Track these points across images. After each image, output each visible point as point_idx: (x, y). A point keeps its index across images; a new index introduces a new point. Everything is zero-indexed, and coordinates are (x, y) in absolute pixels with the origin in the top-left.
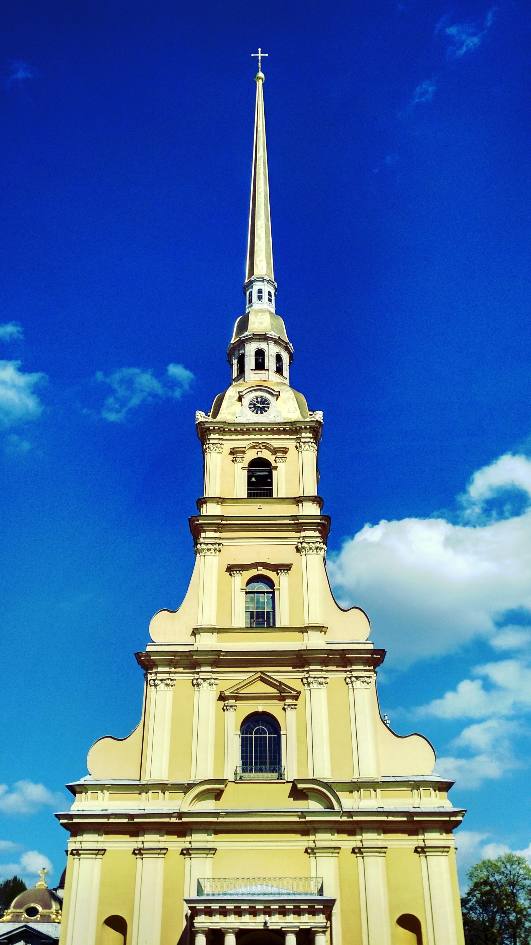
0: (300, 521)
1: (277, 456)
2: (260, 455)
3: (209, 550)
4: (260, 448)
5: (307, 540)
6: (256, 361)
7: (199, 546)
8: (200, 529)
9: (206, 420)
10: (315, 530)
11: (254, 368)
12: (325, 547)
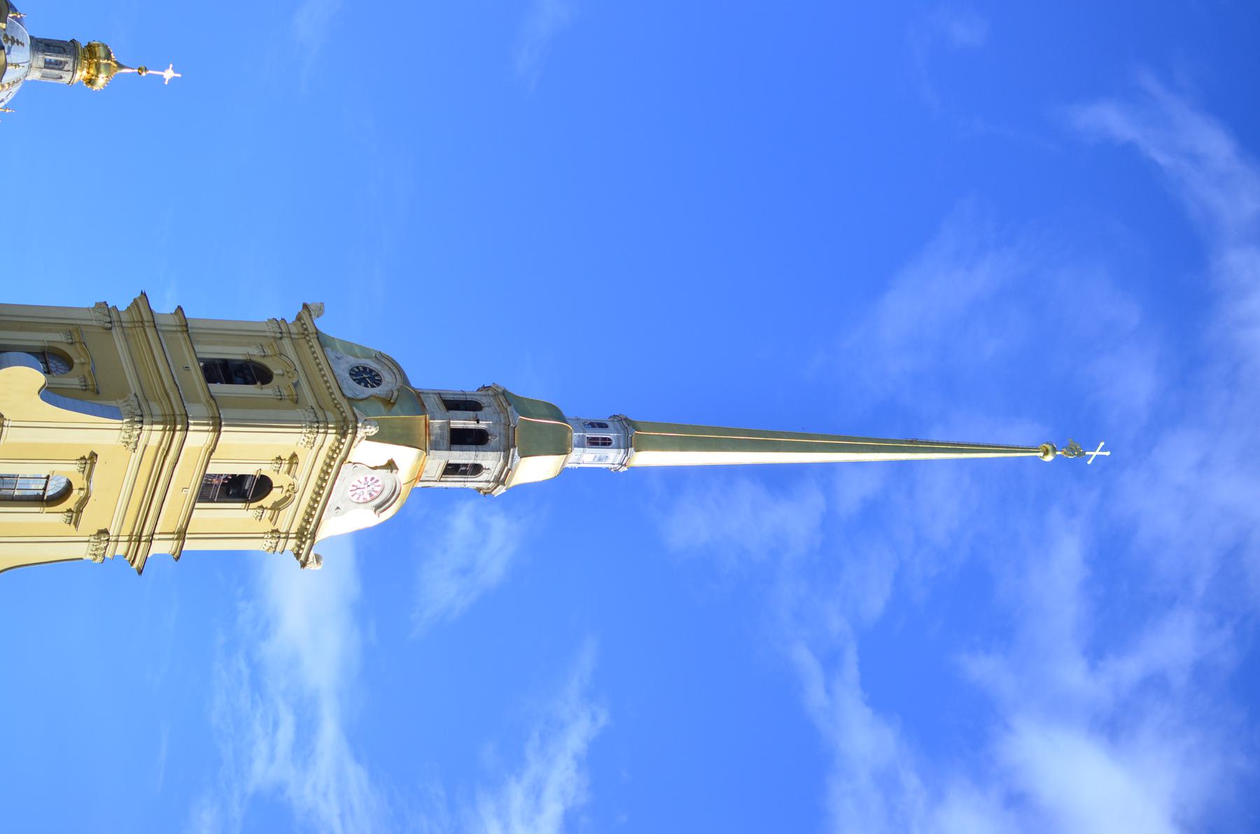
0: (143, 544)
1: (265, 511)
2: (274, 489)
3: (130, 437)
4: (288, 490)
5: (112, 545)
6: (466, 465)
7: (140, 426)
8: (168, 427)
9: (357, 440)
10: (127, 554)
11: (451, 461)
12: (99, 559)
